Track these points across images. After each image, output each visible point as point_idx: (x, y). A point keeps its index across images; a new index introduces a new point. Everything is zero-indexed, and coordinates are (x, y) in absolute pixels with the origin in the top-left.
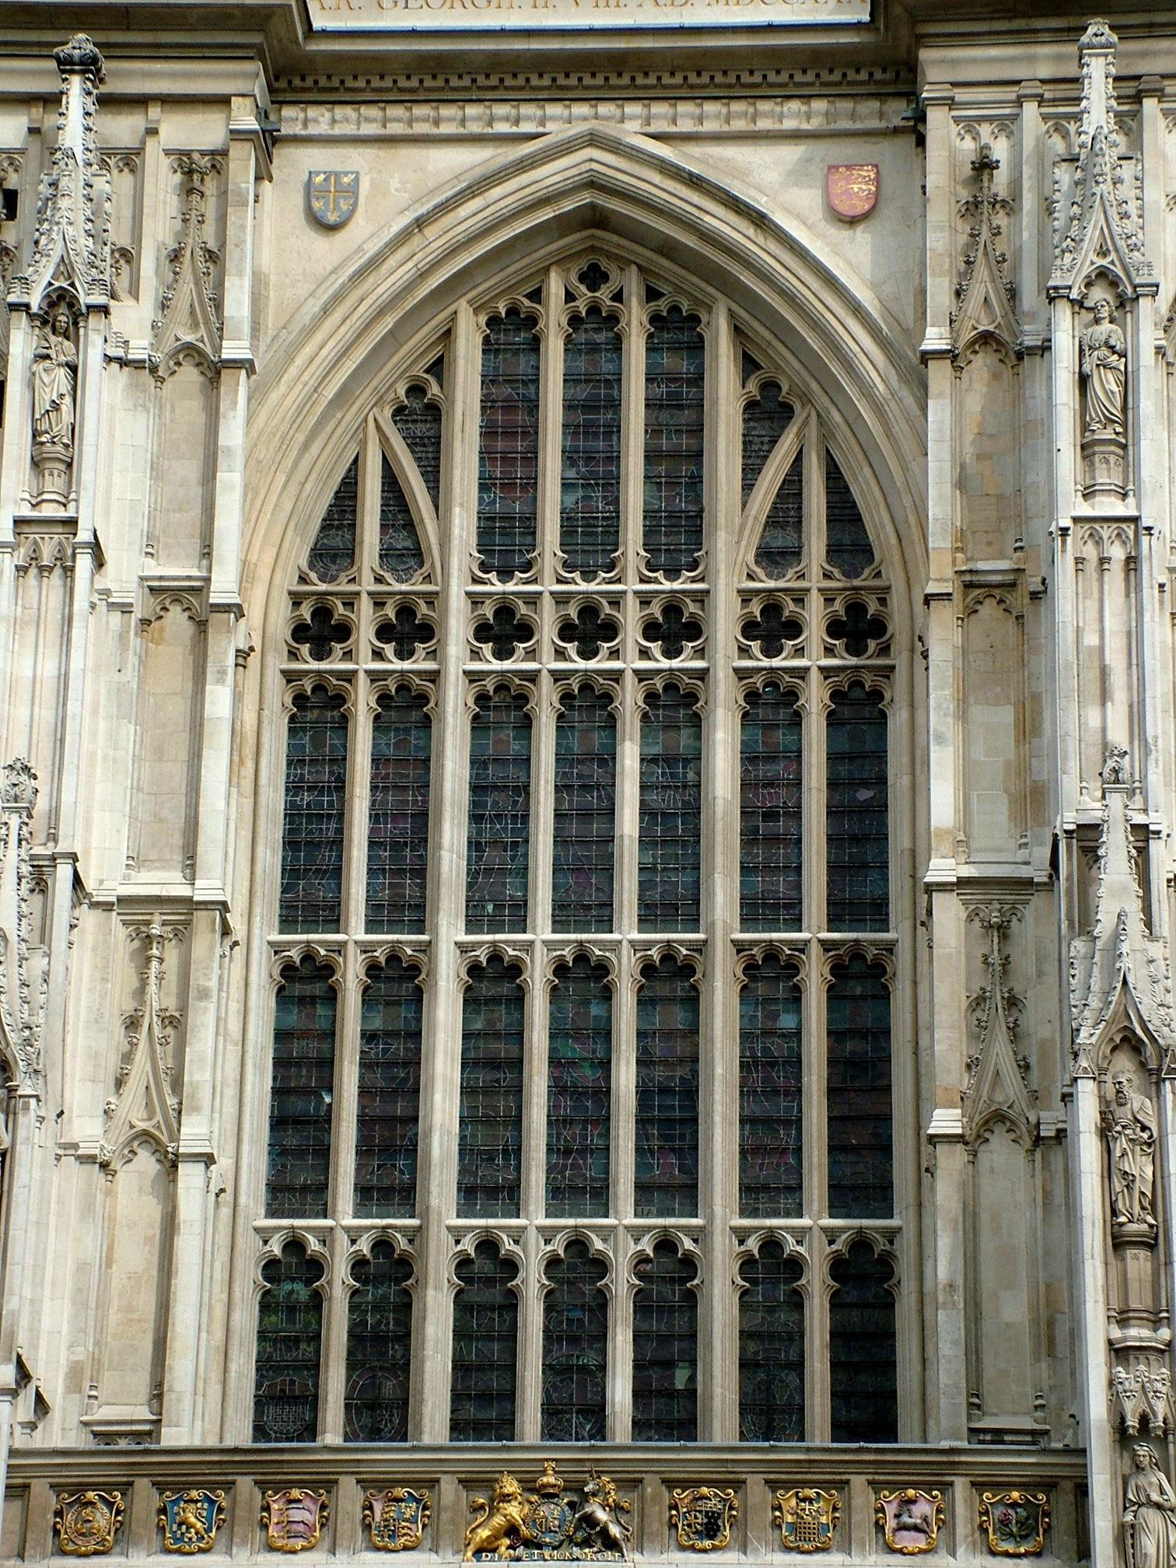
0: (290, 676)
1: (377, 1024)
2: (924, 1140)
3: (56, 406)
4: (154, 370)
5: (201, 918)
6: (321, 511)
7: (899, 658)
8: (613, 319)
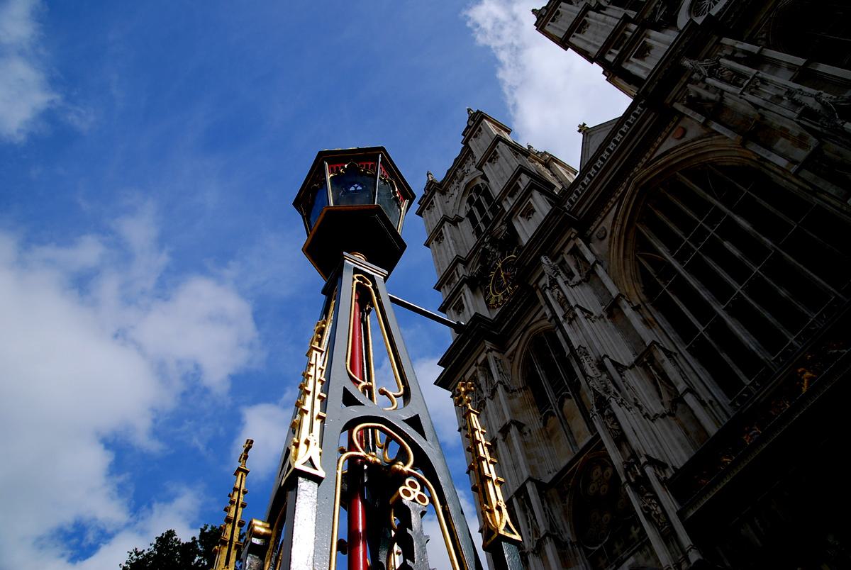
3: (558, 295)
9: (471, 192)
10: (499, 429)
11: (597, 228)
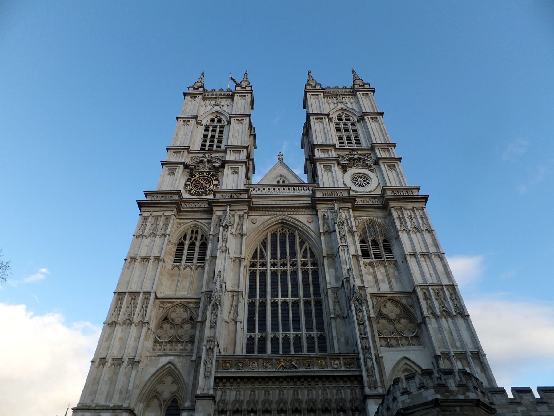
0: (250, 270)
1: (260, 309)
2: (329, 319)
3: (225, 235)
4: (235, 235)
5: (240, 293)
6: (253, 253)
7: (320, 267)
8: (285, 234)
9: (216, 118)
10: (154, 256)
11: (254, 216)
